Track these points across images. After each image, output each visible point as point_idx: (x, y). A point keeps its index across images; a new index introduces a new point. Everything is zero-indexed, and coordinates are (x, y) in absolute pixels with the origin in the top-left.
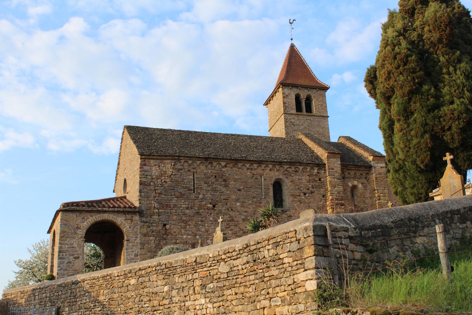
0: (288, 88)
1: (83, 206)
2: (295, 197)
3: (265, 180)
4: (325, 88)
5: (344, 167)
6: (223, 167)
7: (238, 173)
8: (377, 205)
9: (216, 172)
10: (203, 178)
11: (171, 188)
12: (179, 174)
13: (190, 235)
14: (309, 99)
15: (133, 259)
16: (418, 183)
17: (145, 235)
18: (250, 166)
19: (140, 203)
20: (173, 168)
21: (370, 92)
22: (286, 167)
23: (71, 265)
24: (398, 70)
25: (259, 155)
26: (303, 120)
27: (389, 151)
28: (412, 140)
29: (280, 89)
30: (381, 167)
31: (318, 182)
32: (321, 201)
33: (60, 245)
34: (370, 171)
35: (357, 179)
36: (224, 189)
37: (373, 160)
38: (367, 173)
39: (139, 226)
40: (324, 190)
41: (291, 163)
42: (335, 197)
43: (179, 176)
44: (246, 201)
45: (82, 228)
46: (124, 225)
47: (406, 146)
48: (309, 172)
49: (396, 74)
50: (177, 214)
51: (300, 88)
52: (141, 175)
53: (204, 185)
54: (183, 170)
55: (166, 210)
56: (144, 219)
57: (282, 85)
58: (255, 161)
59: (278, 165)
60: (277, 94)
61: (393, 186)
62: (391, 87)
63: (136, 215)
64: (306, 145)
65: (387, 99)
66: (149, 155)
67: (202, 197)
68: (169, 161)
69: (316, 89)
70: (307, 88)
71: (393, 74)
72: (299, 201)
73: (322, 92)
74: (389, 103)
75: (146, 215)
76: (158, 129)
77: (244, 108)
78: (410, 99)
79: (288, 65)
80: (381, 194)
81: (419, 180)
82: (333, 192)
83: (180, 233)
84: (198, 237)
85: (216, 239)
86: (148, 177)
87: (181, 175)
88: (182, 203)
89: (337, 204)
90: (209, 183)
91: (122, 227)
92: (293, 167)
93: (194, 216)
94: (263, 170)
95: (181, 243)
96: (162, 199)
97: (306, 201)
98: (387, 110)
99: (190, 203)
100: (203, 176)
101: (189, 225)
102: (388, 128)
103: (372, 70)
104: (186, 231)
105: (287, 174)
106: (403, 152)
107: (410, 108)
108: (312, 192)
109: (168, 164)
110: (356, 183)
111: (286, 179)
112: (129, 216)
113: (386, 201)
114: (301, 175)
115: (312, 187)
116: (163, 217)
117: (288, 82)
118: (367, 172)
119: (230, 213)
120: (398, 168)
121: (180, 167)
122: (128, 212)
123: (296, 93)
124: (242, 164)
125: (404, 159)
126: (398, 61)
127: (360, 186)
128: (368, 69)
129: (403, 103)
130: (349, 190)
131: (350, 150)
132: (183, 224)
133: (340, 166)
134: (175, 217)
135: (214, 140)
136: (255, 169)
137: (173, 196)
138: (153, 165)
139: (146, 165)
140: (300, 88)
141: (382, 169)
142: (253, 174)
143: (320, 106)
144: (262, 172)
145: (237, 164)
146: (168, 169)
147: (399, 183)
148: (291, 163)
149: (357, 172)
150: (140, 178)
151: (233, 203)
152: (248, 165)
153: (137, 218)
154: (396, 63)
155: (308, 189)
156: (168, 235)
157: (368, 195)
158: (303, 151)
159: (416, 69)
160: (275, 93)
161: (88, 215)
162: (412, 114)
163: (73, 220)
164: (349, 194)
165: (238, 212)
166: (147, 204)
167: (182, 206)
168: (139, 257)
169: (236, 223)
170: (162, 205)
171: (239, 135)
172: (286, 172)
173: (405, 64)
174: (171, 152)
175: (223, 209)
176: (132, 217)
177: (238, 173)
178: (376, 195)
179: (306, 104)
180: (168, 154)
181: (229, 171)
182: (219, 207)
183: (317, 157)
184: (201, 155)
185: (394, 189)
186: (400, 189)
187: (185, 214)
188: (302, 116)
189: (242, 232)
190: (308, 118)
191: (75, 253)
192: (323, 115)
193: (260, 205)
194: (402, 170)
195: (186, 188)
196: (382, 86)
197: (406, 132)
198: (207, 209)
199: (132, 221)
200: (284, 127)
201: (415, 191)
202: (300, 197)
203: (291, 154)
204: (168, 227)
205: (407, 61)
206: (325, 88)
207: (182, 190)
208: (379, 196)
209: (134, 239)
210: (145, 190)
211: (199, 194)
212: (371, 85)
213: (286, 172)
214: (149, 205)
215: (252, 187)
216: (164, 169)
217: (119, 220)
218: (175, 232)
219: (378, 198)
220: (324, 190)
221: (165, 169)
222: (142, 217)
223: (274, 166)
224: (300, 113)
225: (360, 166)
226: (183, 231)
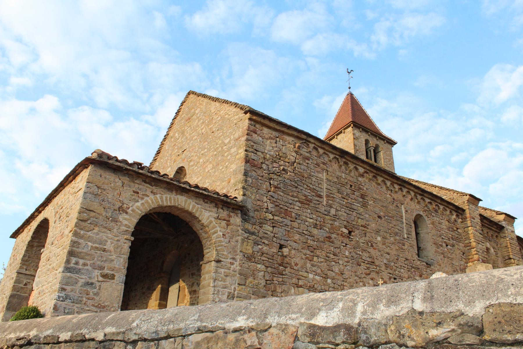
0: (358, 130)
3: (406, 211)
11: (293, 183)
12: (304, 164)
13: (318, 275)
17: (249, 258)
19: (244, 195)
20: (296, 152)
23: (92, 291)
29: (350, 129)
39: (240, 238)
43: (306, 168)
45: (129, 211)
53: (338, 194)
54: (311, 161)
55: (285, 220)
56: (249, 227)
63: (237, 214)
72: (442, 254)
73: (389, 146)
75: (252, 220)
84: (329, 281)
92: (434, 204)
94: (404, 196)
99: (319, 219)
101: (318, 257)
104: (313, 265)
109: (289, 143)
112: (224, 213)
116: (280, 232)
119: (369, 250)
123: (366, 138)
134: (297, 237)
138: (267, 136)
139: (256, 133)
140: (369, 134)
151: (373, 235)
153: (236, 220)
156: (286, 267)
161: (146, 188)
163: (114, 189)
165: (380, 251)
167: (308, 219)
172: (426, 208)
175: (361, 241)
176: (230, 216)
182: (356, 236)
191: (106, 265)
204: (285, 251)
206: (392, 143)
209: (229, 260)
213: (426, 208)
214: (259, 203)
217: (205, 214)
218: (296, 264)
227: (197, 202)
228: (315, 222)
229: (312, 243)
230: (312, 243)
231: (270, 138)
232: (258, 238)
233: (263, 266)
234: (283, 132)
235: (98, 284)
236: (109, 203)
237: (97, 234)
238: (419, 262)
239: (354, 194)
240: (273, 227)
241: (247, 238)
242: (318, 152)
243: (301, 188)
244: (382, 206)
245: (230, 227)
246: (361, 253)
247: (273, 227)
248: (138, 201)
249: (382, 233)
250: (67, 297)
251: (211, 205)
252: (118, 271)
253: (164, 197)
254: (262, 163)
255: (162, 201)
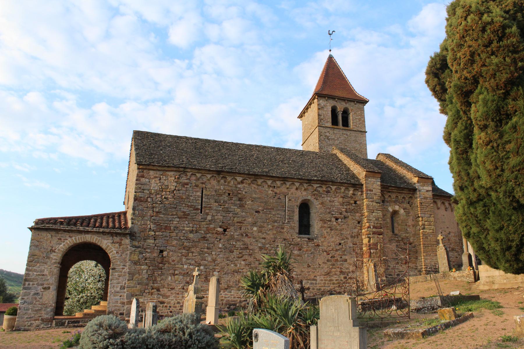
0: (324, 99)
1: (62, 223)
2: (325, 223)
3: (290, 200)
4: (364, 102)
5: (385, 188)
6: (239, 183)
7: (257, 191)
8: (421, 235)
9: (230, 188)
10: (214, 195)
11: (172, 206)
12: (183, 189)
14: (346, 113)
15: (118, 292)
16: (508, 226)
18: (271, 184)
20: (176, 182)
21: (434, 90)
22: (315, 186)
23: (38, 297)
24: (489, 49)
25: (284, 170)
26: (338, 134)
27: (463, 173)
28: (508, 158)
29: (316, 100)
30: (427, 191)
31: (353, 205)
32: (355, 228)
33: (27, 272)
34: (413, 194)
35: (398, 204)
36: (239, 210)
37: (418, 182)
38: (411, 197)
39: (128, 252)
40: (360, 215)
41: (323, 182)
42: (372, 224)
43: (184, 192)
44: (265, 225)
45: (56, 251)
46: (110, 249)
47: (497, 168)
48: (344, 193)
49: (483, 56)
50: (178, 238)
51: (338, 102)
52: (136, 188)
53: (214, 204)
56: (136, 243)
57: (318, 96)
58: (278, 177)
59: (307, 183)
60: (312, 105)
61: (464, 224)
62: (473, 77)
64: (341, 161)
65: (465, 96)
66: (149, 165)
67: (210, 219)
68: (172, 173)
69: (354, 102)
70: (345, 100)
71: (479, 55)
72: (329, 228)
73: (361, 105)
74: (467, 101)
76: (171, 136)
77: (280, 121)
78: (507, 94)
79: (325, 76)
80: (426, 223)
81: (510, 219)
82: (371, 218)
83: (180, 262)
85: (187, 304)
86: (145, 191)
87: (187, 190)
88: (185, 225)
89: (374, 233)
90: (220, 202)
91: (108, 251)
92: (323, 186)
93: (199, 242)
94: (288, 188)
95: (180, 274)
96: (161, 219)
97: (338, 227)
98: (461, 113)
99: (195, 226)
100: (214, 193)
101: (193, 253)
102: (465, 139)
103: (438, 58)
104: (188, 259)
105: (317, 195)
106: (490, 176)
107: (505, 109)
108: (345, 217)
109: (171, 177)
110: (397, 208)
111: (315, 201)
112: (117, 239)
113: (431, 231)
114: (334, 196)
115: (346, 212)
117: (325, 92)
118: (410, 195)
119: (244, 239)
120: (474, 200)
121: (186, 181)
122: (117, 234)
123: (333, 105)
124: (263, 180)
125: (491, 188)
126: (488, 35)
127: (402, 211)
128: (431, 57)
129: (493, 101)
130: (389, 215)
131: (390, 170)
132: (184, 251)
133: (380, 188)
134: (175, 242)
135: (235, 151)
136: (279, 187)
137: (175, 217)
138: (152, 177)
141: (428, 193)
142: (276, 193)
143: (358, 120)
144: (286, 191)
145: (256, 181)
146: (171, 182)
147: (475, 222)
148: (322, 181)
149: (398, 195)
150: (135, 192)
151: (249, 227)
152: (269, 182)
153: (127, 241)
154: (486, 37)
155: (341, 214)
156: (164, 264)
157: (410, 222)
158: (337, 167)
159: (518, 47)
160: (310, 104)
161: (67, 235)
162: (509, 117)
163: (47, 240)
164: (389, 220)
165: (254, 238)
166: (141, 225)
168: (125, 290)
169: (251, 251)
170: (160, 227)
171: (265, 147)
172: (315, 192)
173: (500, 39)
174: (176, 162)
176: (122, 240)
177: (257, 191)
178: (420, 223)
179: (343, 117)
180: (171, 165)
181: (247, 188)
182: (231, 231)
183: (354, 176)
184: (213, 168)
185: (465, 229)
186: (474, 230)
187: (187, 239)
188: (338, 130)
189: (257, 263)
190: (345, 132)
192: (361, 130)
193: (282, 230)
194: (481, 203)
195: (191, 206)
196: (456, 76)
197: (498, 146)
198: (216, 233)
199: (120, 244)
200: (317, 141)
201: (502, 235)
202: (331, 223)
203: (323, 170)
204: (165, 253)
205: (504, 35)
206: (364, 102)
207: (186, 210)
208: (424, 225)
209: (121, 267)
210: (140, 207)
211: (207, 214)
212: (436, 79)
213: (315, 192)
214: (143, 226)
215: (273, 209)
216: (166, 183)
218: (173, 261)
219: (422, 227)
220: (360, 215)
221: (167, 182)
222: (133, 240)
223: (301, 184)
224: (335, 127)
225: (403, 189)
226: (184, 260)
227: (99, 236)
228: (191, 229)
229: (188, 244)
230: (188, 244)
231: (155, 177)
232: (143, 250)
233: (146, 266)
234: (167, 171)
235: (41, 293)
236: (44, 248)
237: (39, 267)
238: (299, 240)
239: (231, 200)
240: (155, 240)
241: (135, 251)
242: (197, 176)
243: (180, 207)
244: (262, 202)
245: (121, 247)
246: (234, 243)
247: (155, 240)
248: (61, 244)
249: (259, 224)
250: (25, 302)
251: (109, 236)
252: (52, 284)
253: (77, 238)
254: (148, 198)
255: (76, 240)
